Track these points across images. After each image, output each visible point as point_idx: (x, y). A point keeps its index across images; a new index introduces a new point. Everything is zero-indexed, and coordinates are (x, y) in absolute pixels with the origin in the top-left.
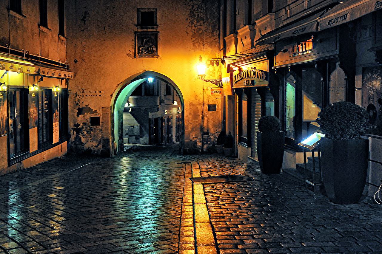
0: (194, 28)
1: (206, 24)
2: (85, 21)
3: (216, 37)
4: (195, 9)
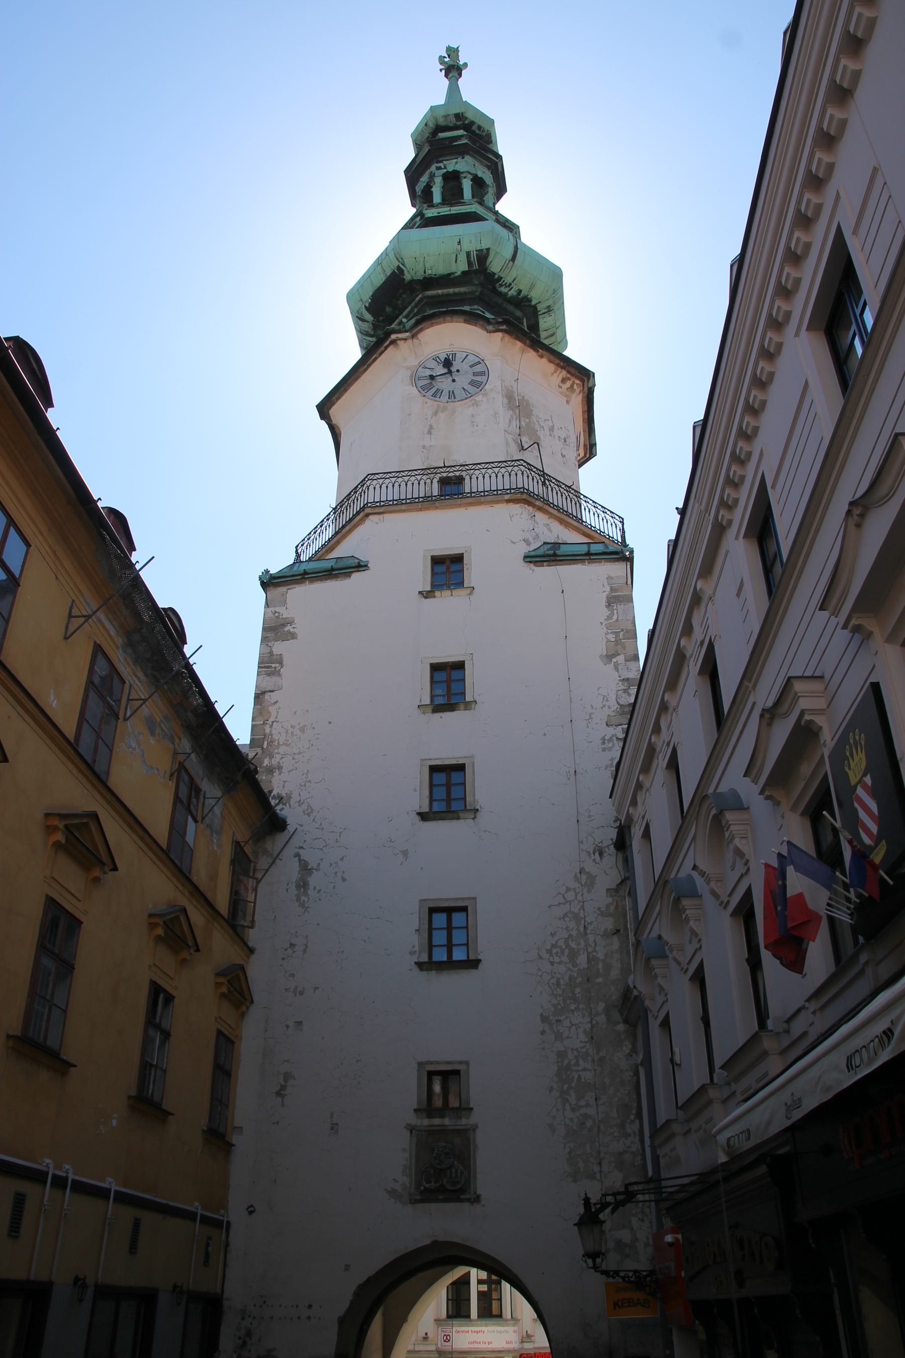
2: (283, 1096)
4: (570, 1061)
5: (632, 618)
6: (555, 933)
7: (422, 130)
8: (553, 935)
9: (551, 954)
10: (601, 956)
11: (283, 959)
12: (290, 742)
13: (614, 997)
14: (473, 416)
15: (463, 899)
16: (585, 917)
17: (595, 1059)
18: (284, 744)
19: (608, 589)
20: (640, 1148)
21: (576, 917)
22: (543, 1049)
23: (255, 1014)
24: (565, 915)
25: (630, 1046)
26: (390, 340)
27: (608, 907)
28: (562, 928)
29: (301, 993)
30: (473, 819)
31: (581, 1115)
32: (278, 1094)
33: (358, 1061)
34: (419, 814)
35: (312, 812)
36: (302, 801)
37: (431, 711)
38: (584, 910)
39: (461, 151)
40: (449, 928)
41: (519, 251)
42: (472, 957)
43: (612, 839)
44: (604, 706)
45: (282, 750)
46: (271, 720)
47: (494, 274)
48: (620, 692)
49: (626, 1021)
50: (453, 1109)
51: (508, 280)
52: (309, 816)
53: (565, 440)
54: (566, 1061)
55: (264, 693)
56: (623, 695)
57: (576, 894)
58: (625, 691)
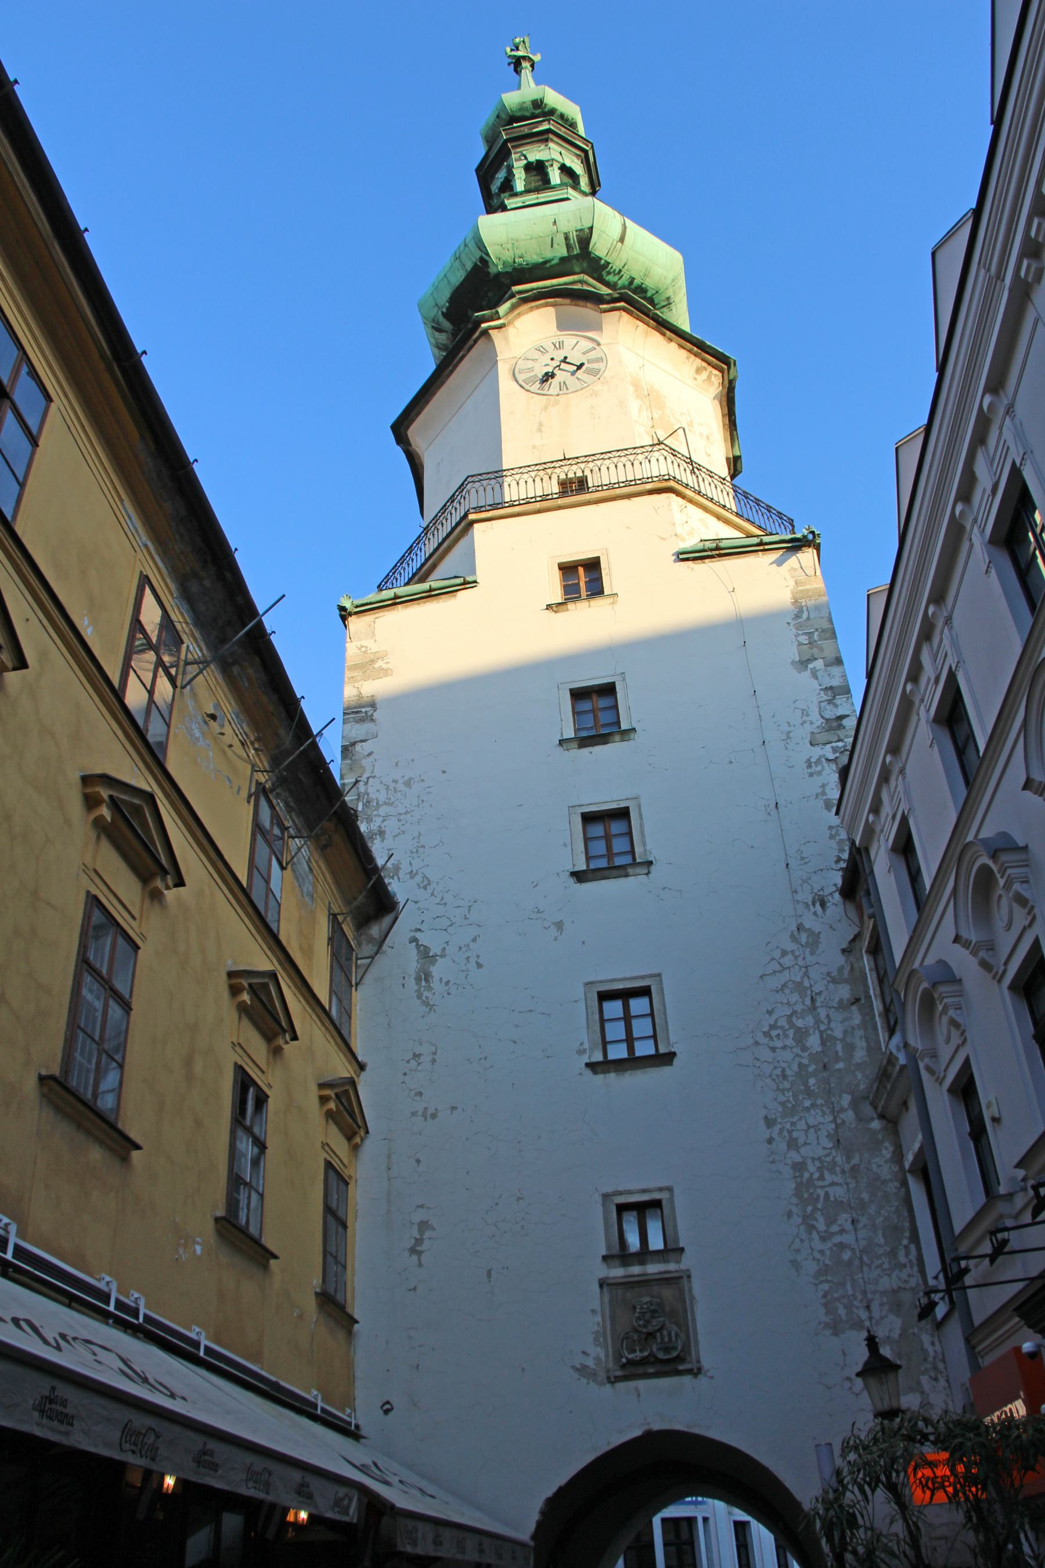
0: (817, 1244)
1: (860, 1225)
2: (419, 1253)
3: (906, 1271)
4: (812, 1174)
5: (827, 615)
6: (773, 1010)
7: (493, 124)
8: (770, 1013)
9: (771, 1038)
10: (838, 1033)
11: (405, 1074)
12: (393, 799)
13: (862, 1087)
14: (592, 407)
15: (642, 977)
16: (811, 986)
17: (846, 1170)
18: (385, 803)
19: (792, 583)
20: (921, 1282)
21: (799, 987)
22: (773, 1162)
23: (370, 1147)
24: (784, 986)
25: (891, 1149)
26: (480, 330)
27: (841, 969)
28: (782, 1003)
29: (434, 1116)
30: (647, 874)
31: (835, 1245)
32: (413, 1251)
33: (519, 1199)
34: (574, 874)
35: (429, 884)
36: (414, 872)
37: (576, 746)
38: (808, 977)
39: (543, 137)
40: (627, 1018)
41: (628, 230)
42: (662, 1050)
43: (835, 885)
44: (805, 722)
45: (383, 811)
46: (364, 778)
47: (601, 259)
48: (823, 704)
49: (882, 1116)
50: (657, 1252)
51: (616, 265)
52: (426, 889)
53: (708, 438)
54: (806, 1175)
55: (353, 744)
56: (828, 707)
57: (796, 958)
58: (830, 702)
